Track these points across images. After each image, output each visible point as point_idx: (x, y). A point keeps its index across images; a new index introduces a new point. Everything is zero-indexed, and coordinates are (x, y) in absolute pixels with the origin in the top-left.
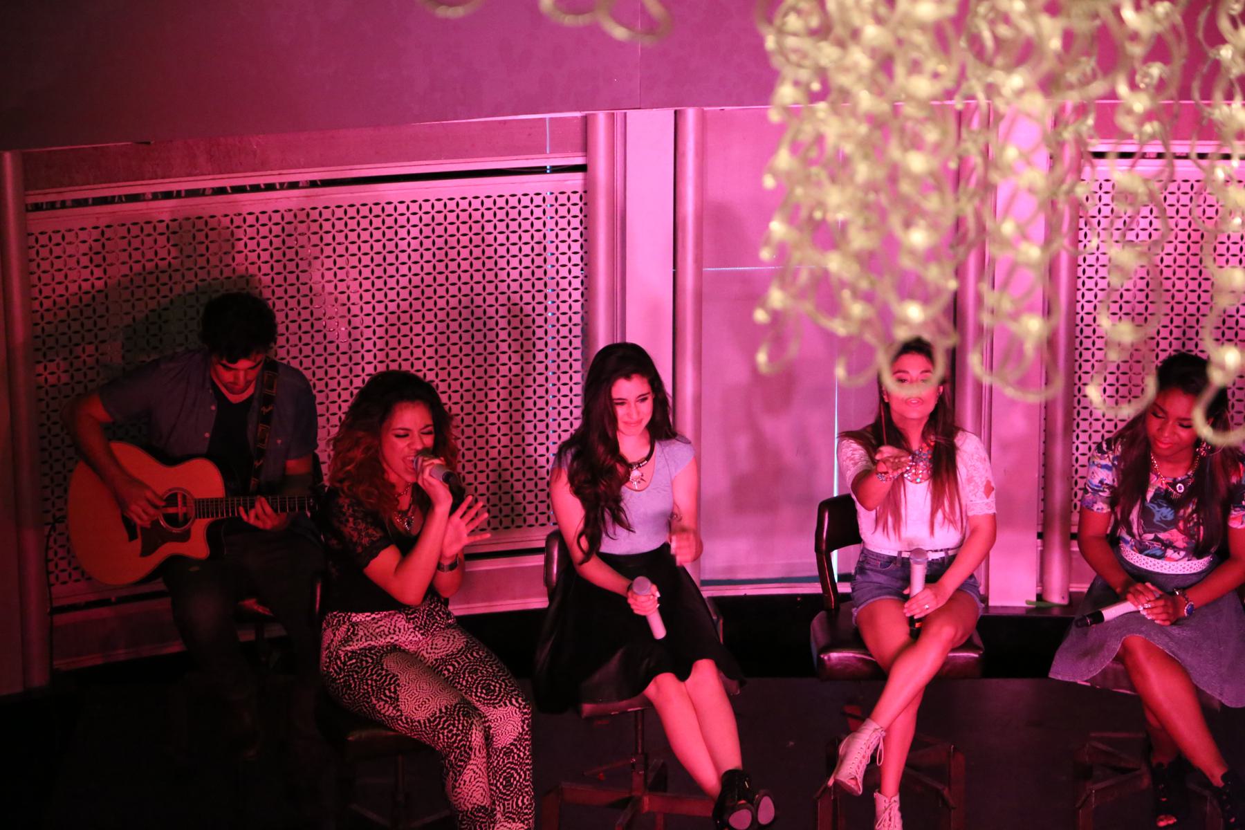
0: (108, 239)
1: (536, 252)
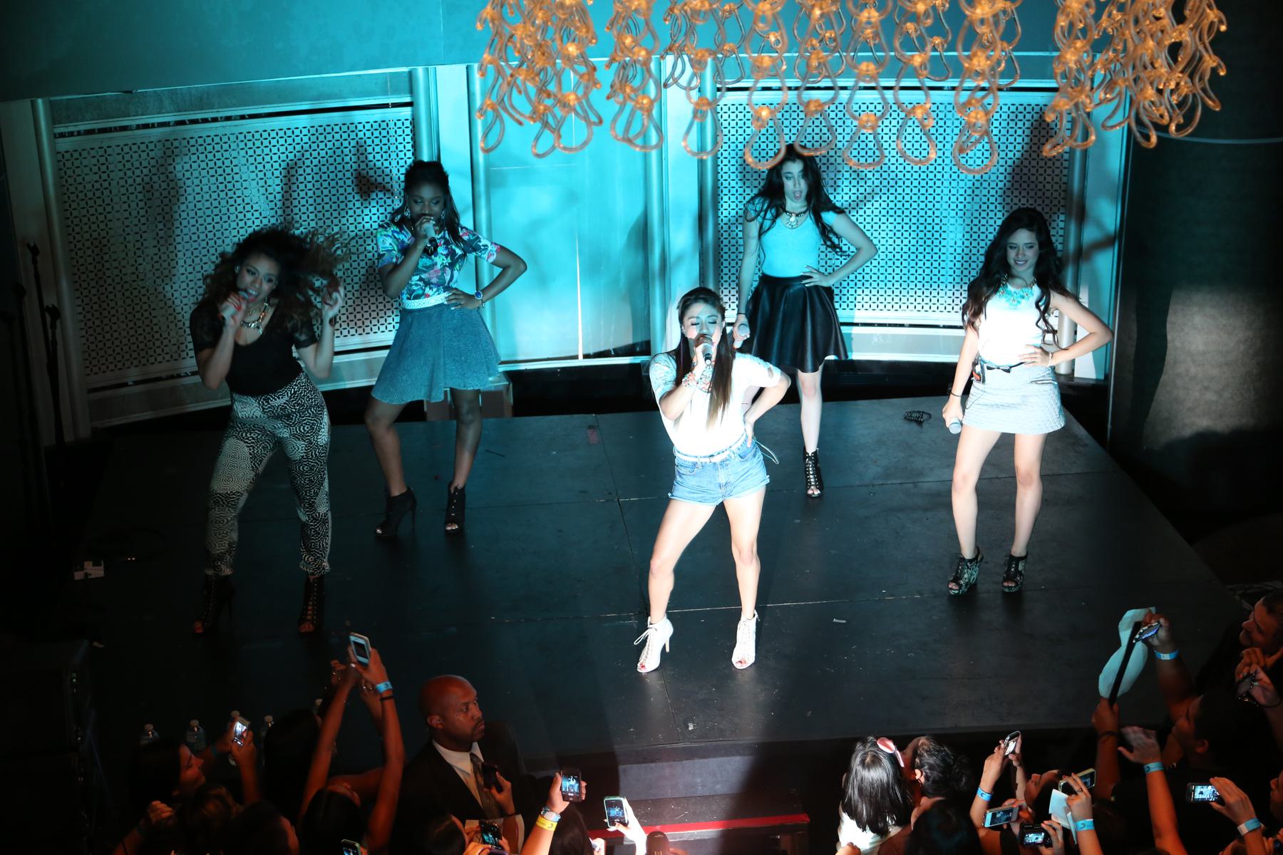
0: (109, 155)
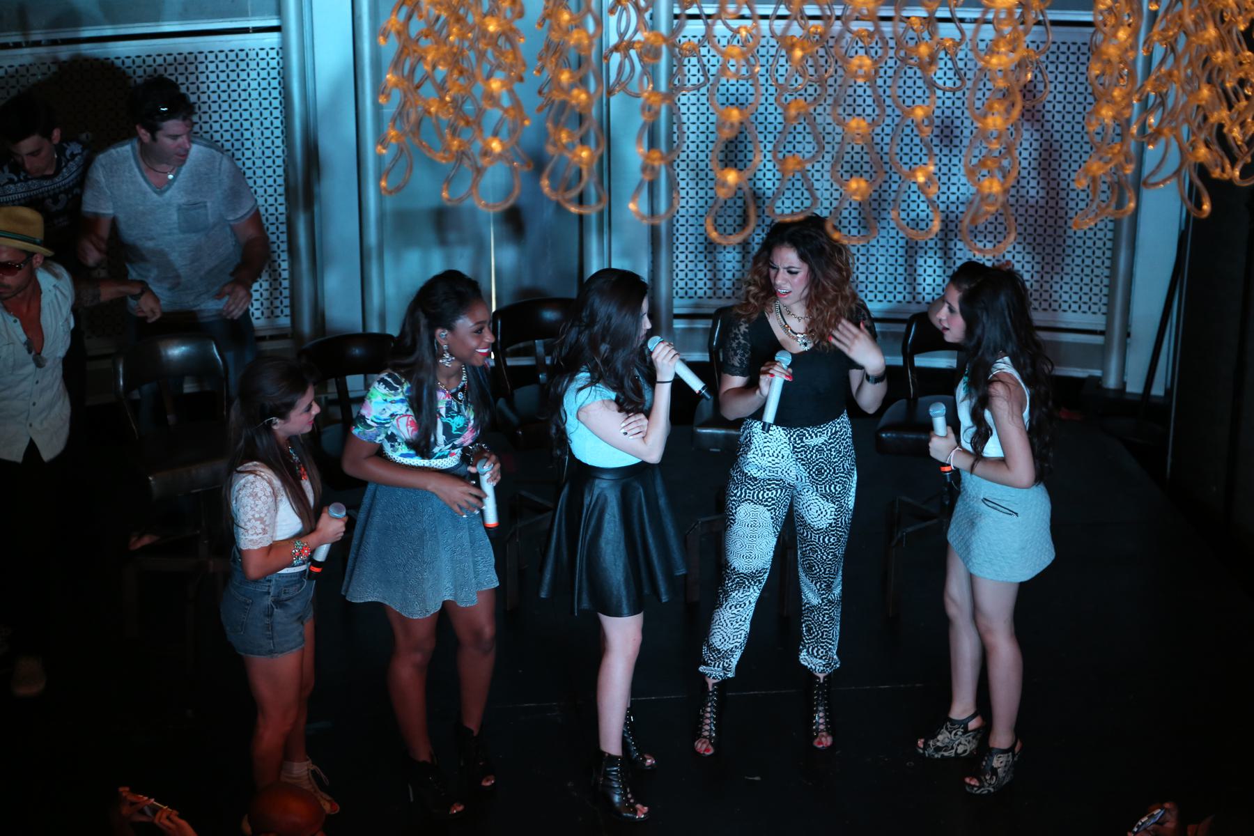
1: (243, 97)
